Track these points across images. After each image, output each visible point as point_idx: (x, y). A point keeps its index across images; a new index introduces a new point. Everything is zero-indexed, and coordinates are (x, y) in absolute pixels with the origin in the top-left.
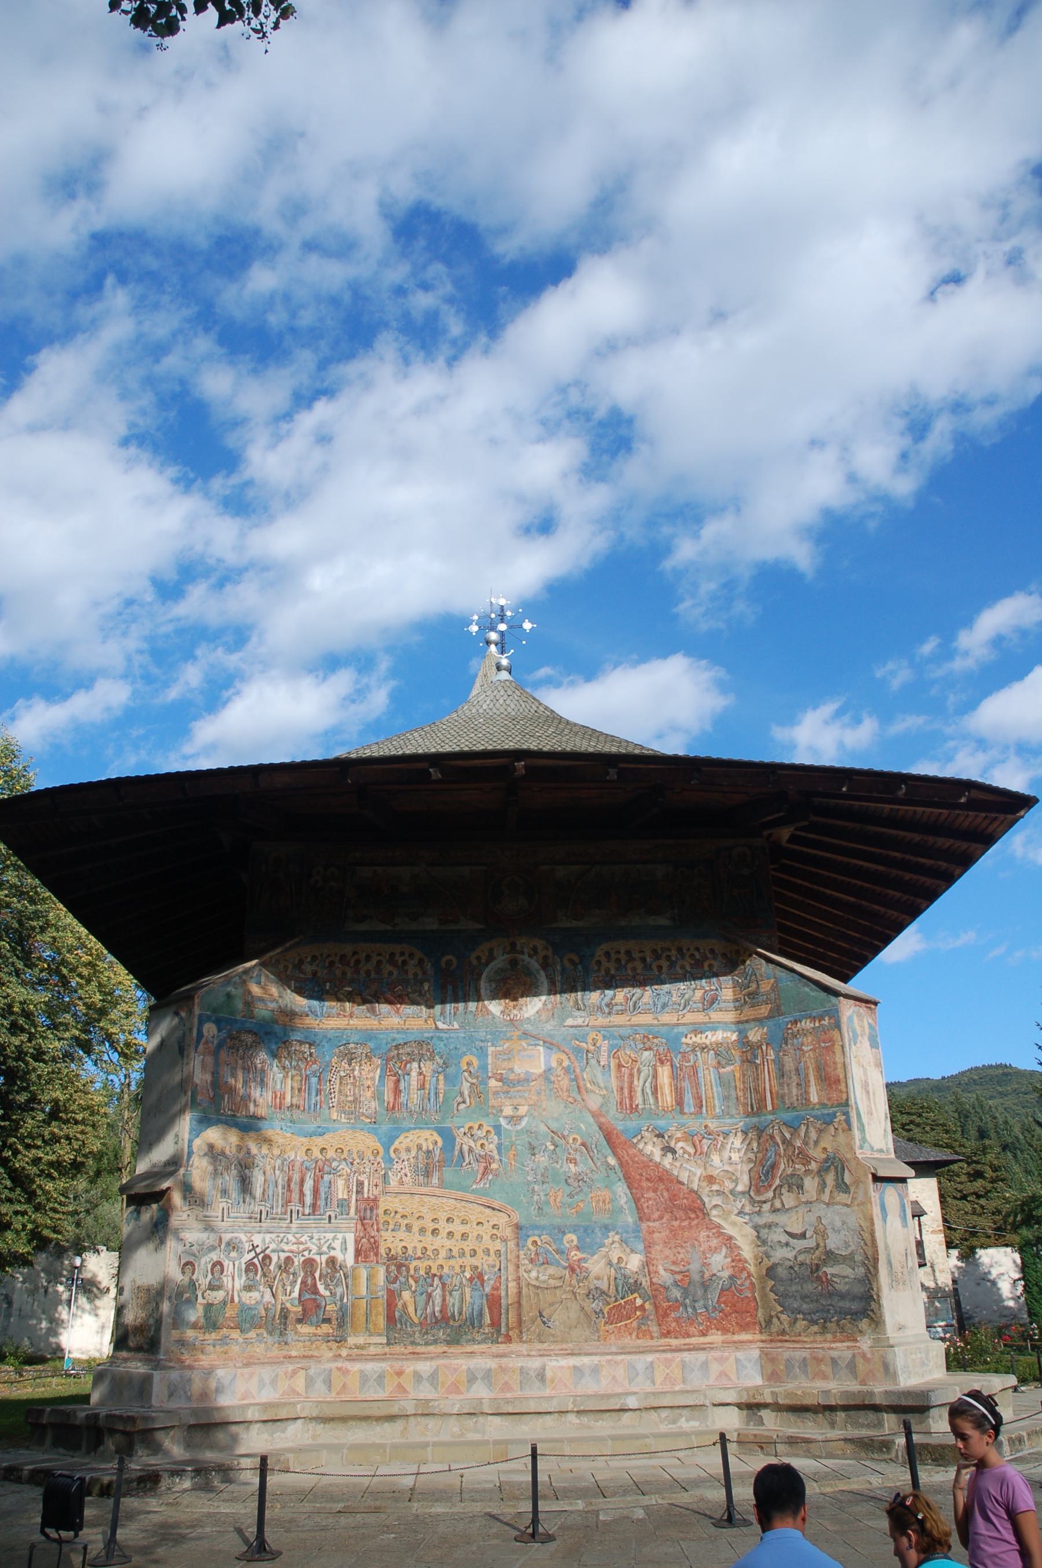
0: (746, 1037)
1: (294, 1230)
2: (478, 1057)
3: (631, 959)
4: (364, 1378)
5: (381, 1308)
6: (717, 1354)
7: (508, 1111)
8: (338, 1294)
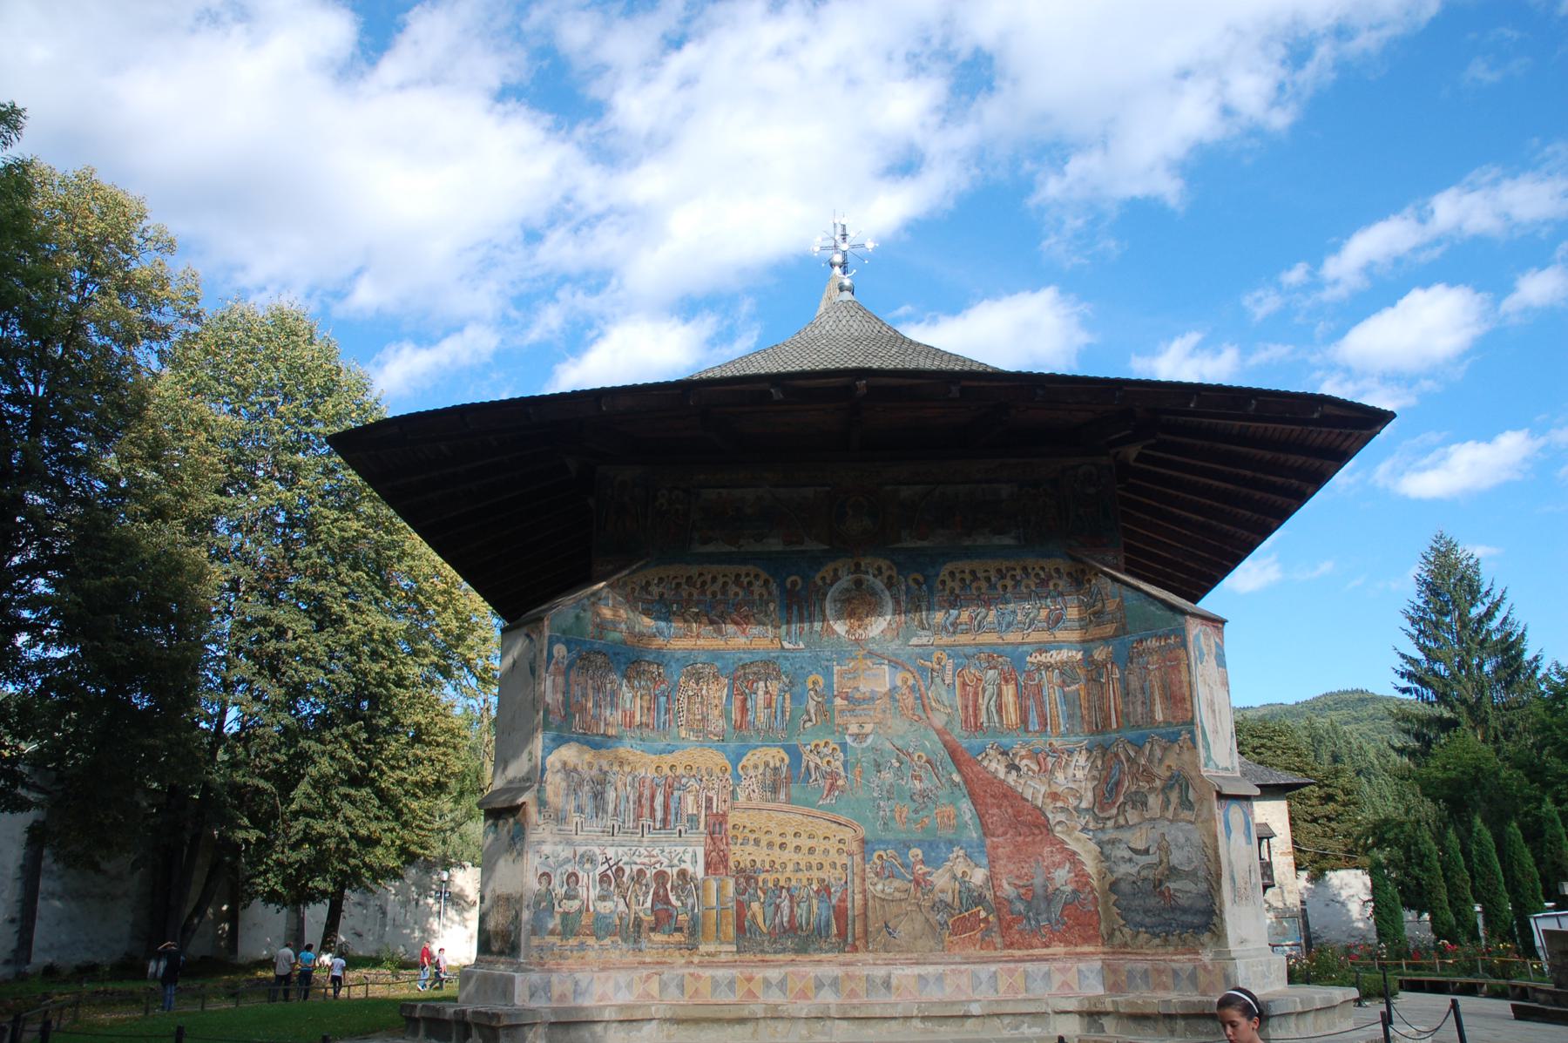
3: (975, 578)
4: (715, 984)
5: (731, 918)
6: (1060, 965)
7: (854, 729)
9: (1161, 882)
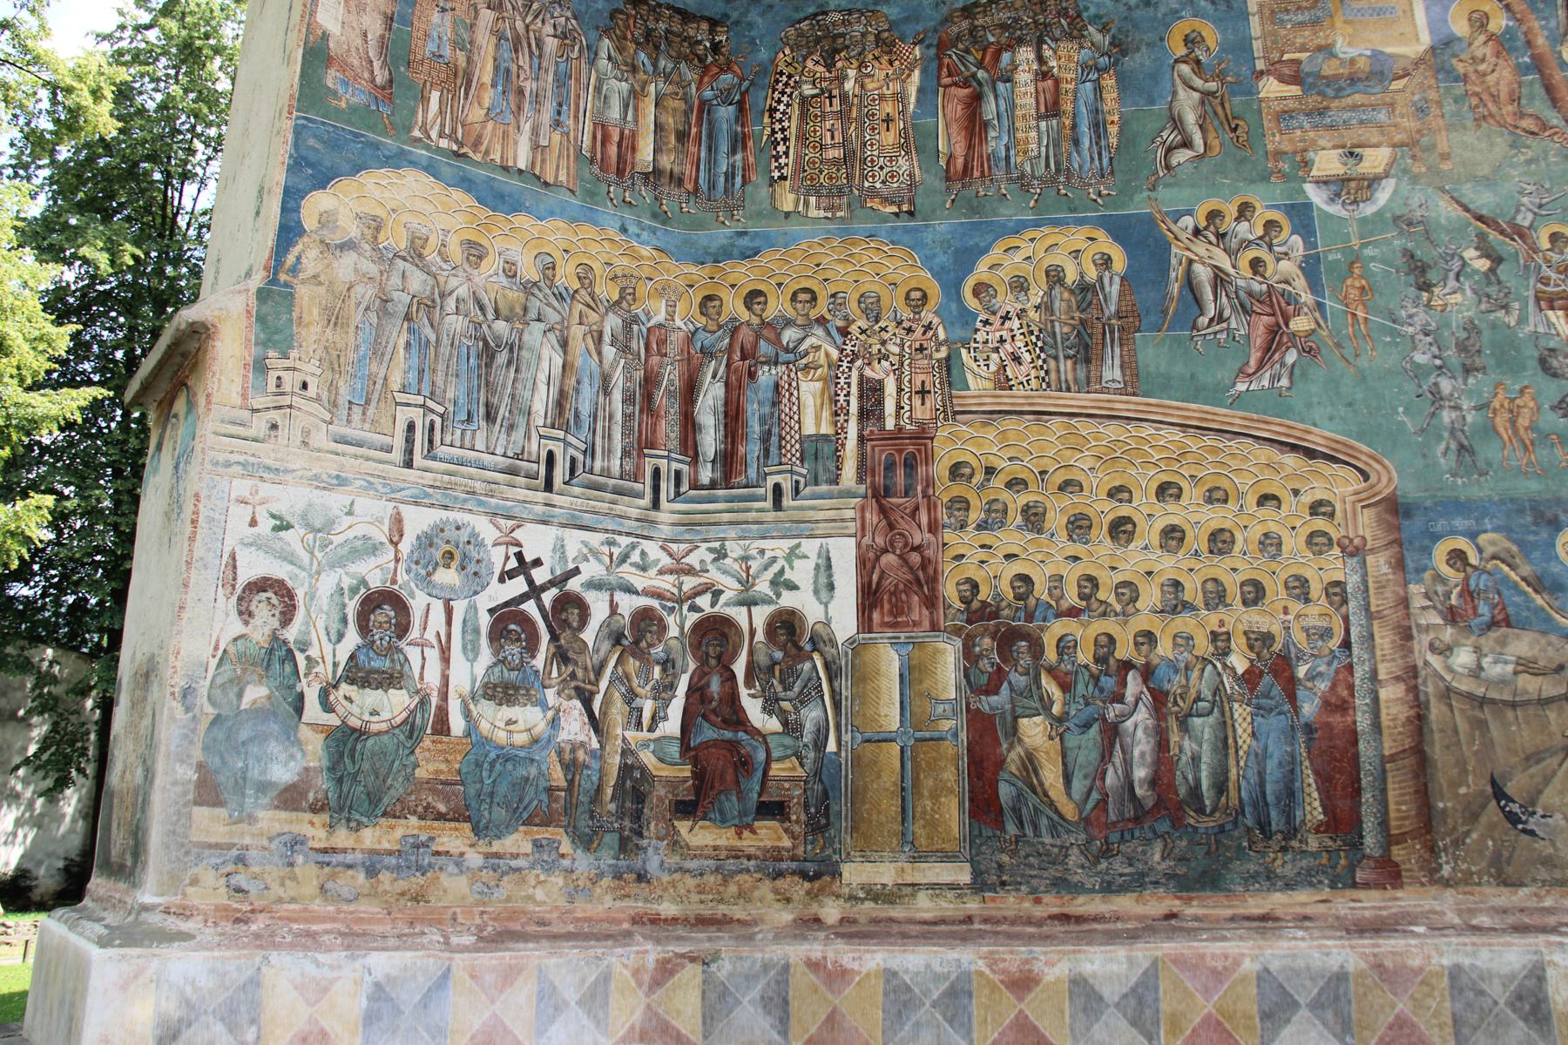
1: (666, 531)
2: (1218, 22)
4: (899, 996)
5: (951, 774)
7: (1328, 162)
8: (809, 727)
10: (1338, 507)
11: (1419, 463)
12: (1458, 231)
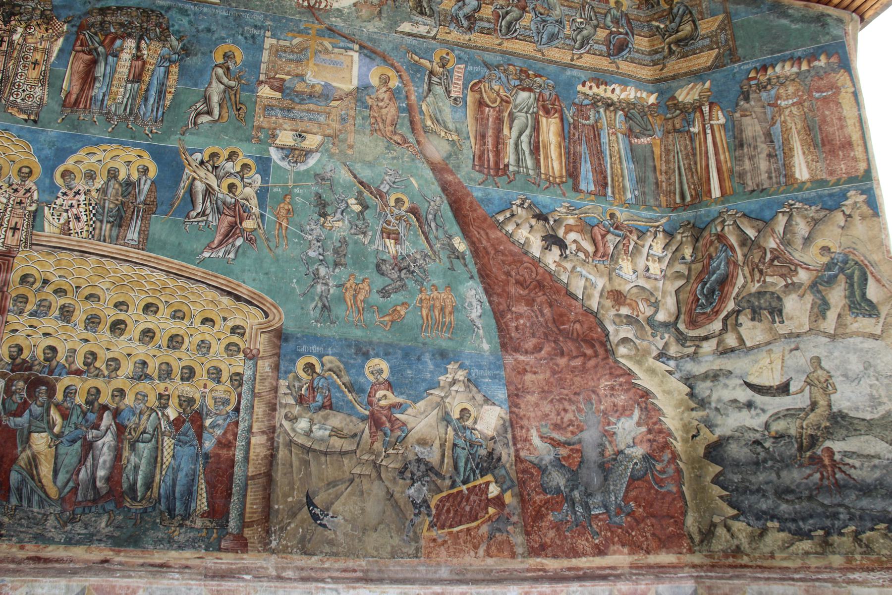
0: (674, 98)
2: (246, 49)
7: (286, 138)
9: (814, 441)
10: (248, 331)
11: (299, 311)
12: (348, 188)
